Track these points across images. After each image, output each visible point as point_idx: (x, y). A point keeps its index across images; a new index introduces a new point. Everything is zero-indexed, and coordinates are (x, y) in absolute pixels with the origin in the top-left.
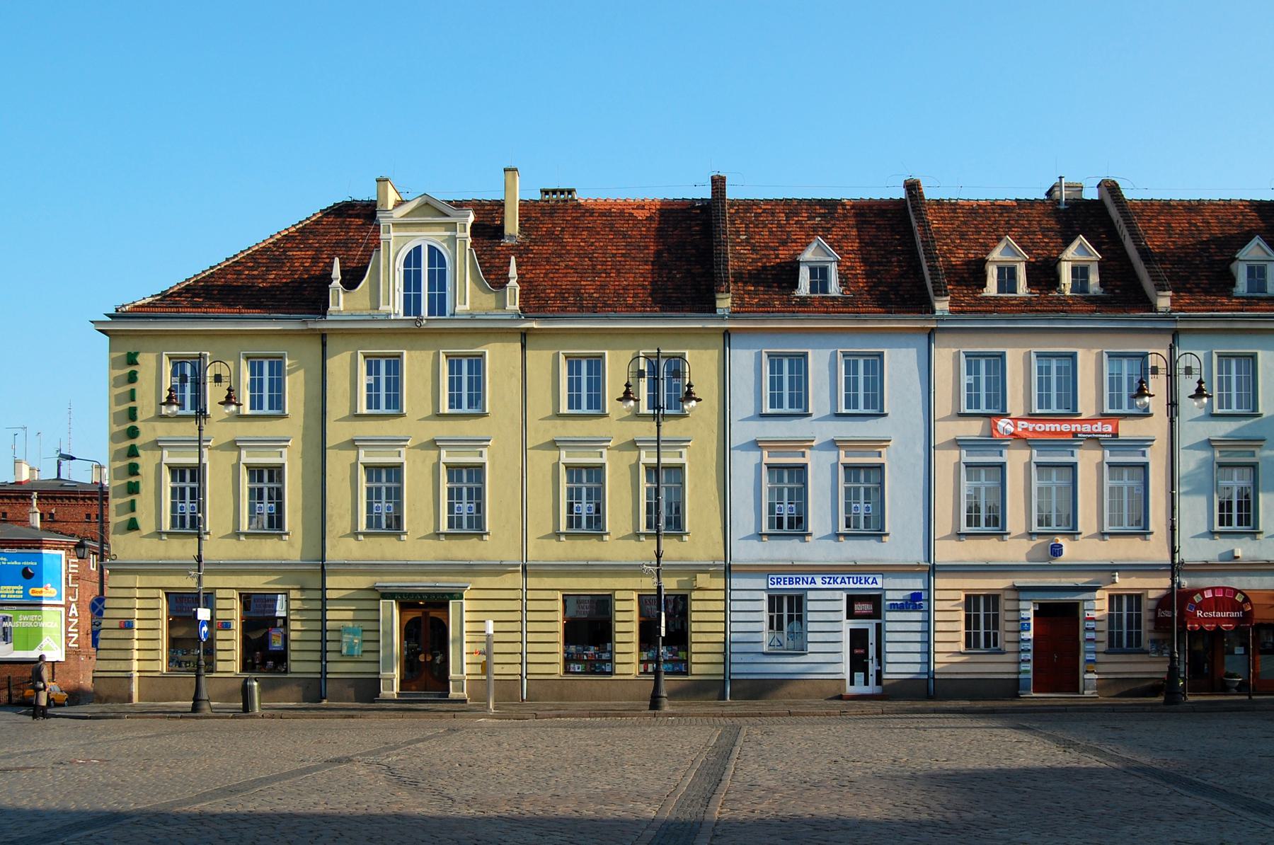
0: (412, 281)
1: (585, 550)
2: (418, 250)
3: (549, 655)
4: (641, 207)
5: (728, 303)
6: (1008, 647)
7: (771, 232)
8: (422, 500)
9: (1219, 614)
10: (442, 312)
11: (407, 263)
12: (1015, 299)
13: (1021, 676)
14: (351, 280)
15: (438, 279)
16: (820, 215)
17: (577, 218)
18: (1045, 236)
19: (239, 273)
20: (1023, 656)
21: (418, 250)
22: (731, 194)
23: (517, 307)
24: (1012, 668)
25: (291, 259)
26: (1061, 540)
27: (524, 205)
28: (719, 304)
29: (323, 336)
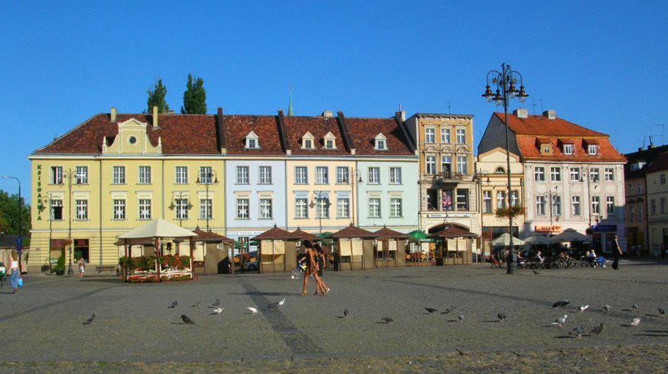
8: (132, 210)
14: (110, 141)
22: (224, 113)
25: (86, 134)
28: (223, 152)
29: (100, 160)
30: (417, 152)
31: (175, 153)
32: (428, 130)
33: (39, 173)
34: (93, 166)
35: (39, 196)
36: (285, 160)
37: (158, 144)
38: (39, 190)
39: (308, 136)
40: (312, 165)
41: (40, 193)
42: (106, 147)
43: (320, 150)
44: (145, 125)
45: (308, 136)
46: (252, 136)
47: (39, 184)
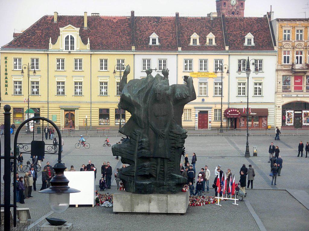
0: (67, 42)
1: (104, 99)
2: (68, 36)
3: (96, 121)
4: (115, 18)
5: (134, 48)
6: (193, 120)
7: (144, 27)
8: (69, 89)
9: (234, 115)
10: (73, 49)
11: (66, 39)
12: (196, 46)
13: (196, 126)
14: (54, 42)
15: (72, 42)
16: (156, 22)
17: (100, 22)
18: (206, 28)
19: (26, 37)
20: (196, 122)
21: (68, 36)
22: (135, 15)
23: (89, 49)
24: (194, 124)
26: (204, 98)
27: (88, 17)
28: (132, 48)
29: (48, 54)
30: (276, 48)
31: (99, 50)
32: (285, 31)
33: (6, 62)
34: (43, 59)
35: (6, 78)
36: (177, 55)
37: (87, 43)
38: (6, 74)
39: (195, 36)
40: (196, 58)
41: (7, 76)
42: (52, 45)
43: (203, 48)
44: (79, 29)
45: (195, 36)
46: (154, 36)
47: (6, 70)
